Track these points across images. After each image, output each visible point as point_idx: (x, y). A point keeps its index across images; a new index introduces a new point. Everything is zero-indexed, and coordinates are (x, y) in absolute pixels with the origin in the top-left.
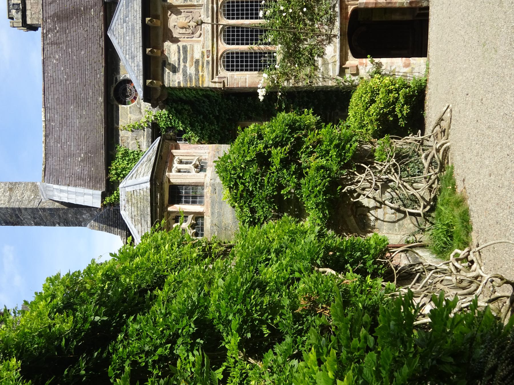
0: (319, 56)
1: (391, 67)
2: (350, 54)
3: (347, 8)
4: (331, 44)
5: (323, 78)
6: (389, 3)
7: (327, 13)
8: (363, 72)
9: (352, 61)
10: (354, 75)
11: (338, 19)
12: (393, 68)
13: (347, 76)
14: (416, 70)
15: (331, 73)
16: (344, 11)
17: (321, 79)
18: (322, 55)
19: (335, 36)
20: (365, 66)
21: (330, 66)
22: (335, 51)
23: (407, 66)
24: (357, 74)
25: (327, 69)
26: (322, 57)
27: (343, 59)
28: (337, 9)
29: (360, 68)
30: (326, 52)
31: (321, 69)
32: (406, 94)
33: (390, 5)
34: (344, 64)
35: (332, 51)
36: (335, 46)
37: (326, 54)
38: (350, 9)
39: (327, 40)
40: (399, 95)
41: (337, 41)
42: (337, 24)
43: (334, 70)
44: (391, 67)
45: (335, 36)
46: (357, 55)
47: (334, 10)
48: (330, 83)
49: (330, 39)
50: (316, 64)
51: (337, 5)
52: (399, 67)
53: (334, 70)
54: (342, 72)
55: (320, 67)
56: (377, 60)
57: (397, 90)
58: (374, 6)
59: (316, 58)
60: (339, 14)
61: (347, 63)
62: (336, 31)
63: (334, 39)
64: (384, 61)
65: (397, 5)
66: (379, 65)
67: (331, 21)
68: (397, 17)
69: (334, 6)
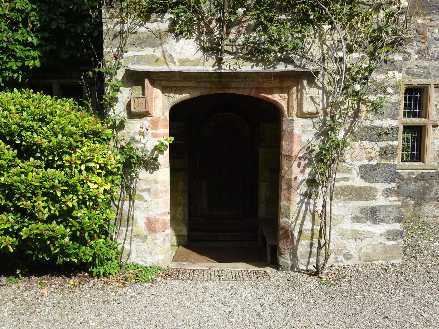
0: (174, 23)
1: (148, 190)
2: (178, 97)
3: (281, 90)
4: (200, 53)
5: (121, 33)
6: (290, 187)
7: (272, 42)
8: (133, 127)
9: (161, 103)
10: (129, 105)
11: (259, 69)
12: (145, 195)
13: (125, 94)
14: (143, 246)
15: (131, 52)
16: (275, 83)
17: (118, 28)
18: (177, 31)
19: (219, 61)
20: (152, 133)
21: (148, 51)
22: (183, 62)
23: (151, 226)
24: (132, 115)
25: (141, 43)
26: (171, 30)
27: (166, 81)
28: (281, 67)
29: (146, 122)
30: (182, 41)
31: (142, 29)
32: (52, 239)
33: (284, 186)
34: (153, 83)
35: (185, 54)
36: (197, 62)
37: (178, 40)
38: (278, 98)
39: (211, 41)
40: (49, 220)
41: (209, 66)
42: (247, 67)
43: (139, 59)
44: (148, 190)
45: (219, 61)
46: (176, 112)
47: (280, 60)
48: (109, 50)
49: (213, 49)
50: (154, 16)
51: (290, 68)
52: (147, 209)
53: (139, 58)
54: (135, 78)
55: (148, 25)
56: (164, 159)
57: (65, 216)
58: (285, 152)
59: (168, 16)
60: (271, 70)
61: (157, 92)
62: (230, 64)
63: (212, 61)
64: (163, 174)
65: (283, 203)
66: (151, 165)
67: (254, 52)
68: (263, 191)
69: (288, 61)
